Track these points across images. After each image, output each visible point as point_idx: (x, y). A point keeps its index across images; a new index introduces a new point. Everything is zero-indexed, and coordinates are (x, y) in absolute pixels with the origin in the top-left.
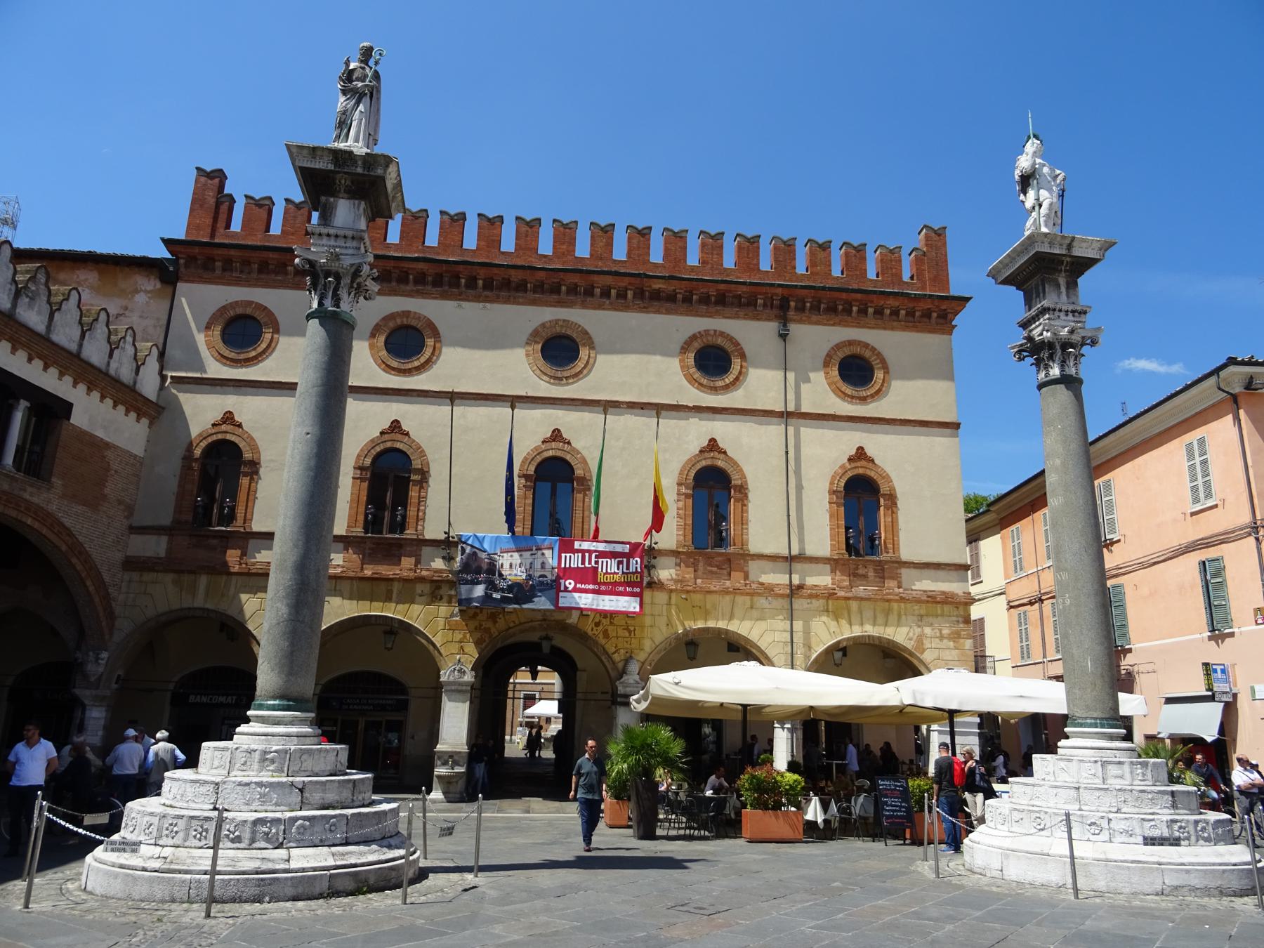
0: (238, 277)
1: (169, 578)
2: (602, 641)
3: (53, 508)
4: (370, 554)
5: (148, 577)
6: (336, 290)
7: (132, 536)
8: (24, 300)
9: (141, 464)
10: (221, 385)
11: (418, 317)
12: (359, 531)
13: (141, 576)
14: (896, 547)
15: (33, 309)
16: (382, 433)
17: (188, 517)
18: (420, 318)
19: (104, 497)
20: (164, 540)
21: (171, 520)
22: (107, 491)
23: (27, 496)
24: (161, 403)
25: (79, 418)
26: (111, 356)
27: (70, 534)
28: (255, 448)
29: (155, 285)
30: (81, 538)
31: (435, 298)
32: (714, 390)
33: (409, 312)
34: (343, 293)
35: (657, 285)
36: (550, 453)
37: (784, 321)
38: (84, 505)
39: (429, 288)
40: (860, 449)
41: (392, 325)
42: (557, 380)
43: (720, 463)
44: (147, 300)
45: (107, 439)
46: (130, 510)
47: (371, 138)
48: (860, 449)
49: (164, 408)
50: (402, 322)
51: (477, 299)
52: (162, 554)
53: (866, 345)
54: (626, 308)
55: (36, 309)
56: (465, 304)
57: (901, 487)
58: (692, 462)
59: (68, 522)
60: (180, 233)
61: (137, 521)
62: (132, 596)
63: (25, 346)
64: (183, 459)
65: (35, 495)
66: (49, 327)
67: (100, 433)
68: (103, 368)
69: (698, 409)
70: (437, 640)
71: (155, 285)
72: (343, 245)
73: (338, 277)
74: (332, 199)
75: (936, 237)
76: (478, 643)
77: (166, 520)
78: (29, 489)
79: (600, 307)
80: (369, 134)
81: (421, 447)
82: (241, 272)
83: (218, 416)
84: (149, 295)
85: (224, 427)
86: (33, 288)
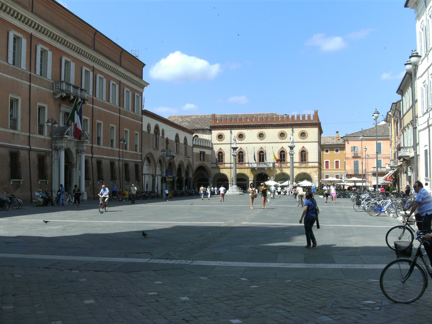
1: (216, 169)
2: (268, 174)
5: (214, 169)
11: (242, 133)
14: (308, 160)
20: (215, 164)
25: (206, 153)
32: (282, 139)
35: (274, 125)
36: (261, 150)
37: (293, 128)
40: (303, 147)
42: (261, 140)
43: (283, 150)
46: (211, 161)
48: (303, 147)
51: (250, 129)
53: (305, 131)
54: (269, 128)
56: (249, 130)
57: (309, 151)
58: (279, 150)
59: (207, 165)
65: (205, 163)
69: (280, 143)
70: (248, 175)
75: (316, 113)
76: (253, 175)
77: (215, 162)
79: (266, 128)
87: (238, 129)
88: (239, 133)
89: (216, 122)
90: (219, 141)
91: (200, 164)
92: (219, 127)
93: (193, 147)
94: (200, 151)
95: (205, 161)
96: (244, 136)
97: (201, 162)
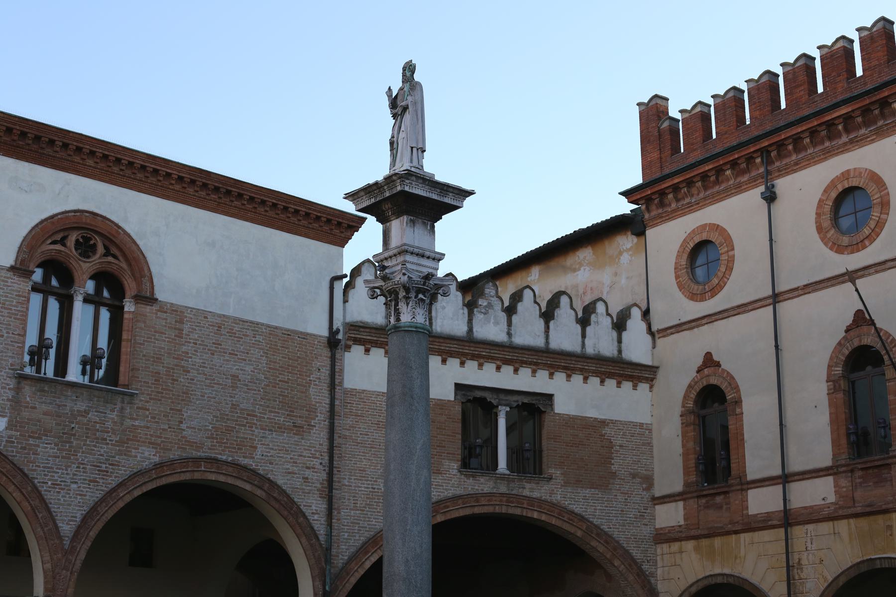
0: (689, 203)
1: (690, 545)
3: (557, 497)
4: (861, 483)
5: (675, 546)
6: (397, 305)
7: (657, 507)
8: (478, 317)
9: (650, 431)
10: (698, 326)
11: (858, 172)
12: (844, 458)
13: (670, 547)
15: (489, 322)
16: (847, 331)
17: (693, 478)
18: (861, 173)
19: (614, 475)
21: (682, 484)
22: (614, 468)
23: (526, 493)
24: (656, 364)
25: (563, 406)
26: (584, 336)
27: (582, 518)
28: (737, 389)
29: (633, 241)
30: (596, 521)
31: (873, 141)
33: (848, 171)
34: (402, 306)
38: (591, 488)
39: (863, 131)
41: (834, 195)
44: (630, 257)
45: (603, 417)
46: (648, 481)
47: (415, 150)
49: (657, 368)
50: (843, 186)
52: (682, 523)
55: (492, 321)
59: (577, 508)
60: (637, 179)
61: (658, 492)
62: (666, 568)
63: (490, 359)
64: (681, 416)
65: (532, 490)
66: (509, 334)
67: (592, 413)
68: (577, 349)
71: (633, 241)
72: (396, 263)
73: (397, 294)
74: (388, 224)
77: (678, 487)
78: (528, 486)
80: (412, 148)
81: (890, 335)
82: (692, 196)
83: (699, 361)
84: (630, 253)
85: (706, 371)
86: (485, 304)
87: (828, 154)
88: (833, 184)
89: (667, 152)
90: (694, 297)
91: (455, 499)
92: (690, 183)
93: (333, 343)
94: (458, 387)
95: (556, 472)
96: (876, 197)
97: (483, 485)
